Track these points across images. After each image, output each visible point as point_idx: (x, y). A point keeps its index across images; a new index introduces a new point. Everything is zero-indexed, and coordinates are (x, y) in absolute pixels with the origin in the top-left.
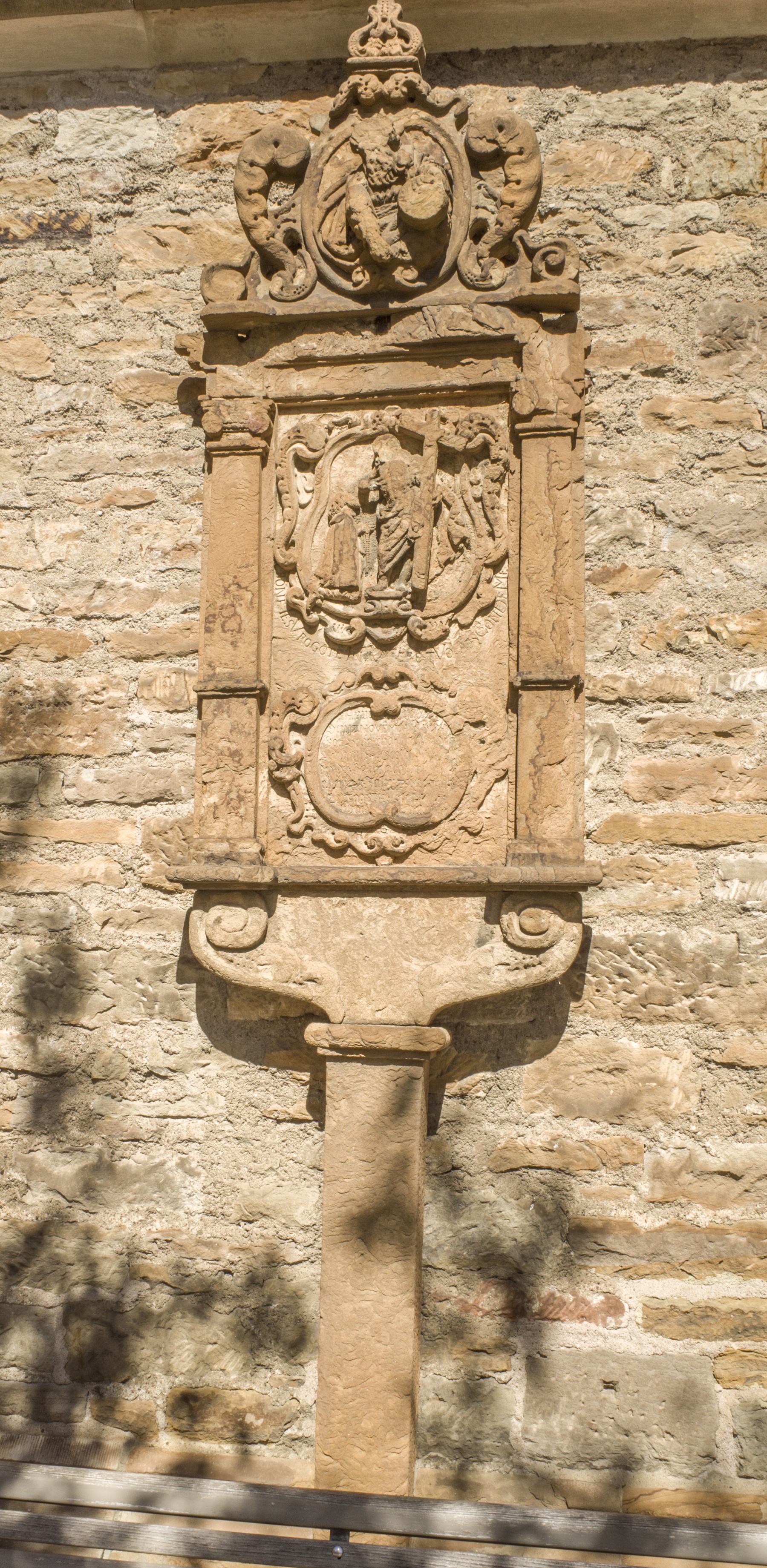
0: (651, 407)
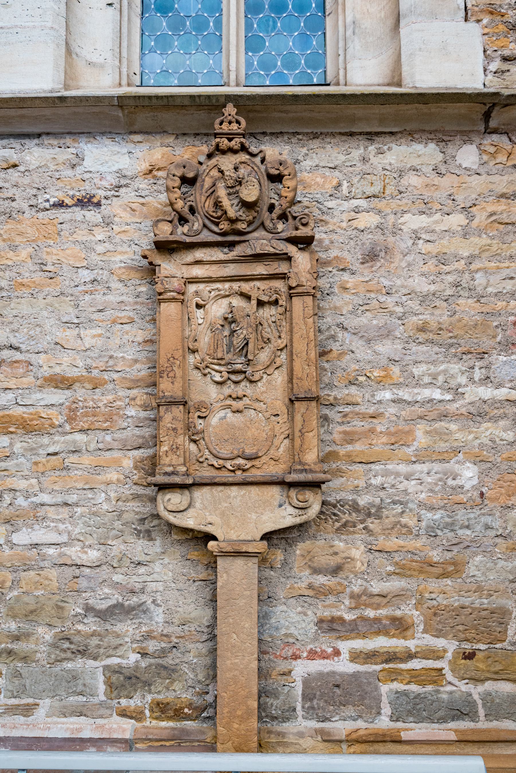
0: (341, 284)
